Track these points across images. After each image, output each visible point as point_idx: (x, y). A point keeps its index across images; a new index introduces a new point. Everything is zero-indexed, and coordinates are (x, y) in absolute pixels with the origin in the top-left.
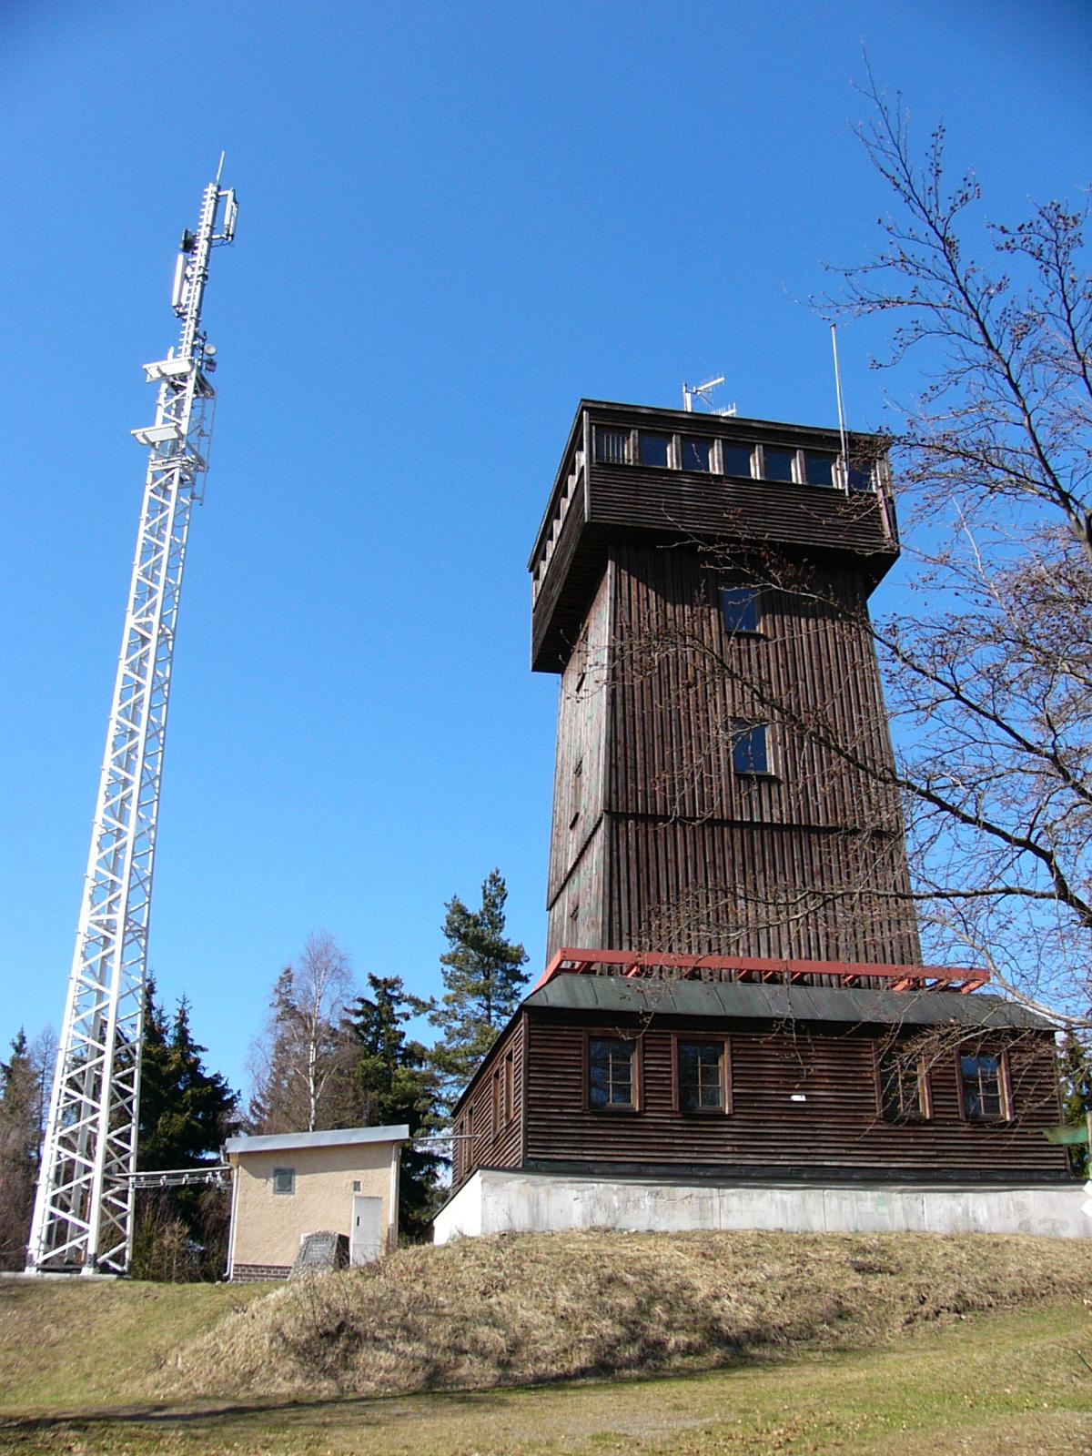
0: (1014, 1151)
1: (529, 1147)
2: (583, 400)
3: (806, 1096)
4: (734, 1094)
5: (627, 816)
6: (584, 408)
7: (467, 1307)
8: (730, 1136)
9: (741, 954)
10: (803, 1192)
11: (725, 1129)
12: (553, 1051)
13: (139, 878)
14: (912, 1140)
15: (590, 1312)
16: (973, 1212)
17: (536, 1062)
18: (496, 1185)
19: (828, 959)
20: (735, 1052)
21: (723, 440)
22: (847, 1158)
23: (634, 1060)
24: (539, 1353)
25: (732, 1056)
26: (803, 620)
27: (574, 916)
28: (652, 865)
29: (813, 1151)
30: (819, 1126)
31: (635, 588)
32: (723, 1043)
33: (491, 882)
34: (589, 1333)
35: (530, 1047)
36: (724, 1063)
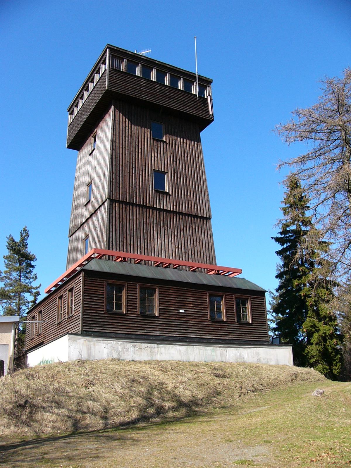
0: (252, 334)
1: (84, 326)
2: (108, 44)
3: (185, 311)
4: (160, 309)
5: (116, 201)
6: (108, 47)
7: (80, 392)
8: (158, 325)
9: (156, 256)
10: (187, 346)
11: (157, 322)
12: (93, 288)
14: (220, 329)
15: (131, 394)
16: (243, 355)
17: (87, 292)
18: (74, 341)
19: (185, 260)
20: (160, 292)
21: (156, 69)
22: (198, 334)
23: (124, 294)
24: (117, 413)
25: (159, 294)
26: (179, 138)
27: (86, 238)
28: (124, 221)
29: (187, 331)
30: (189, 322)
31: (121, 117)
32: (156, 289)
33: (24, 231)
34: (134, 403)
35: (85, 286)
36: (156, 296)
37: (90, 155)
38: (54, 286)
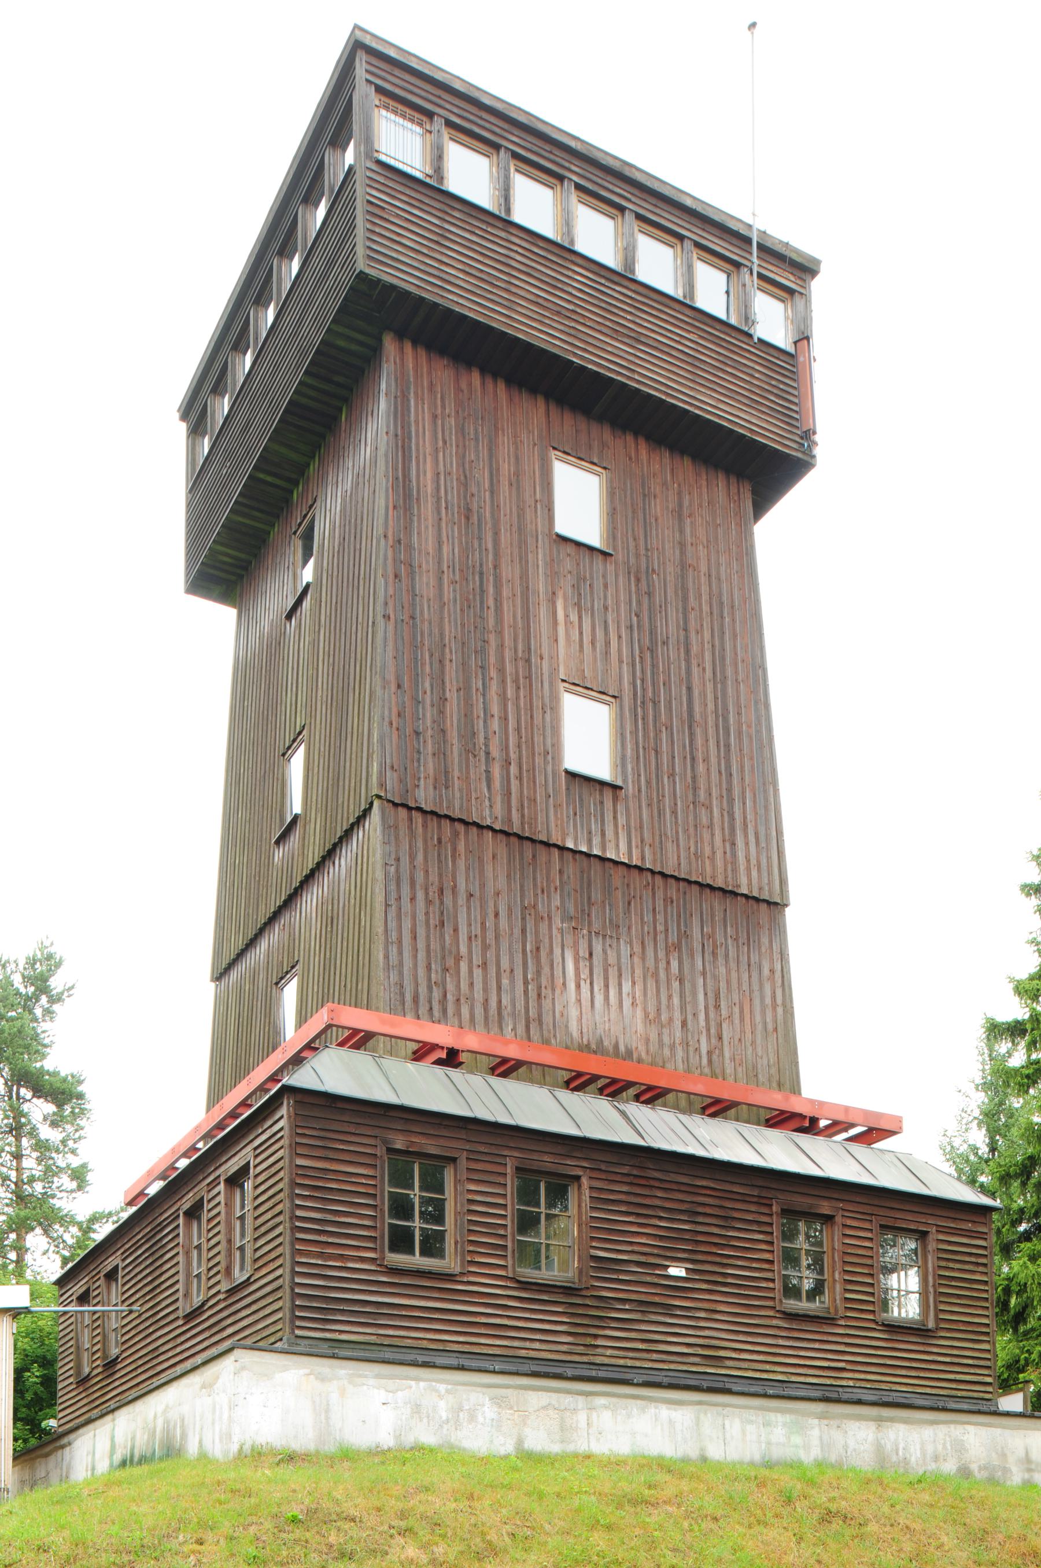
32: (578, 1178)
38: (185, 1155)
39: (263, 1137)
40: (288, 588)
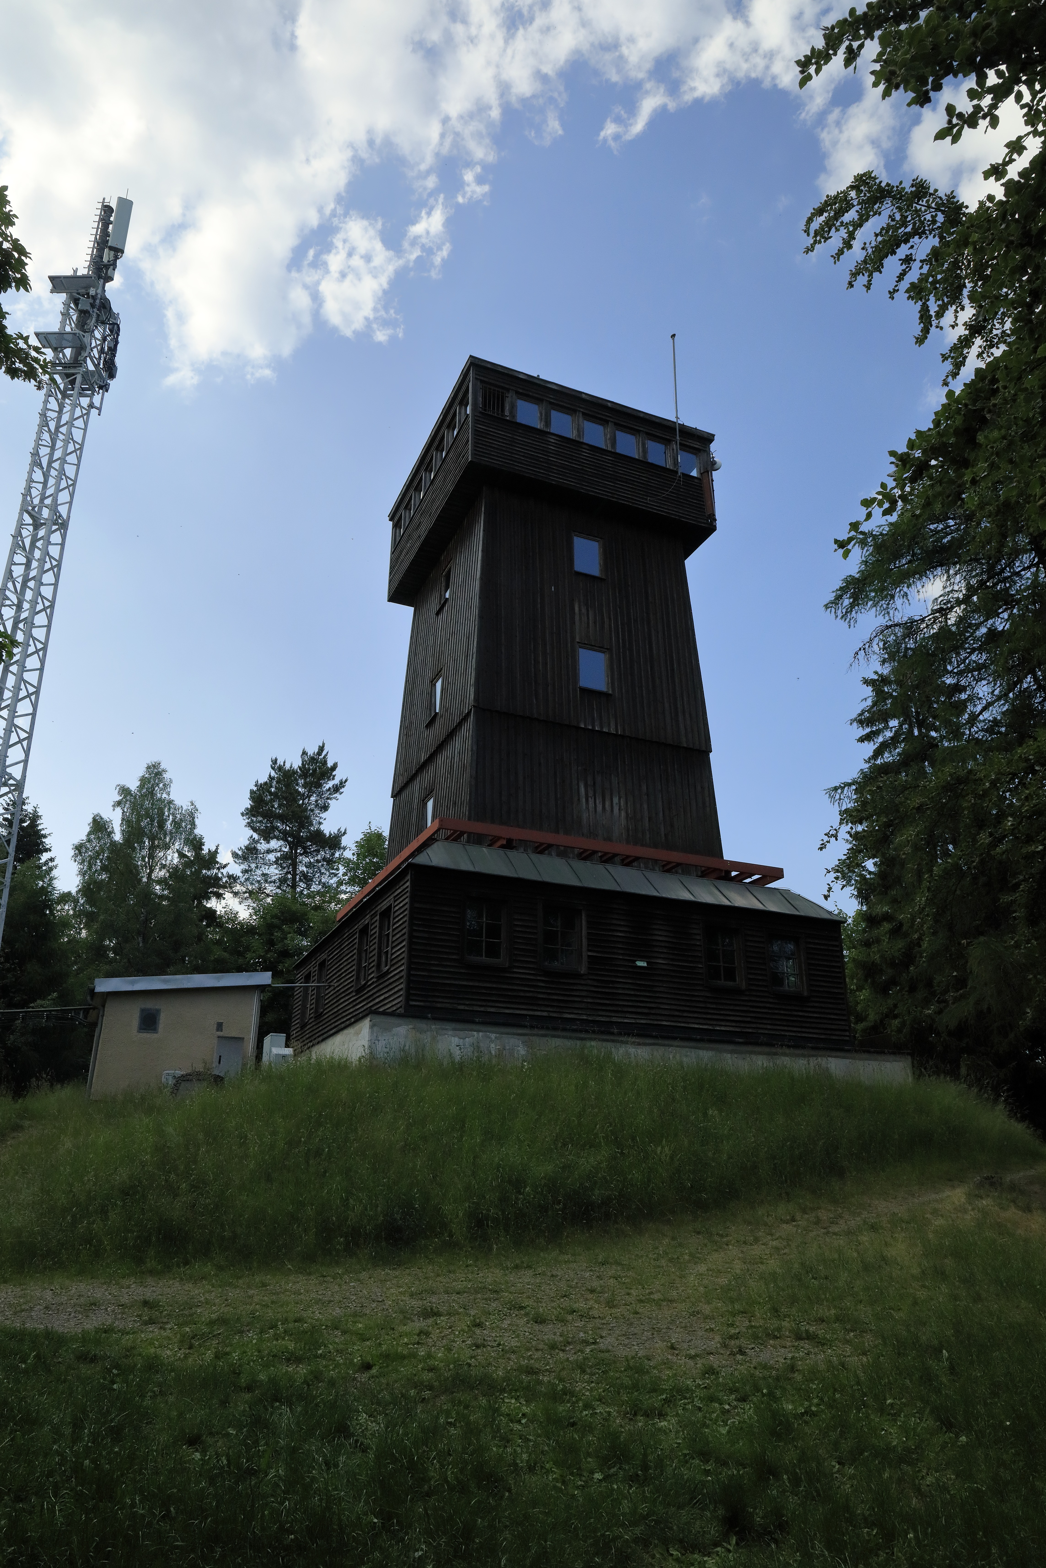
3: (648, 963)
13: (19, 737)
37: (438, 613)
39: (399, 891)
40: (437, 601)
